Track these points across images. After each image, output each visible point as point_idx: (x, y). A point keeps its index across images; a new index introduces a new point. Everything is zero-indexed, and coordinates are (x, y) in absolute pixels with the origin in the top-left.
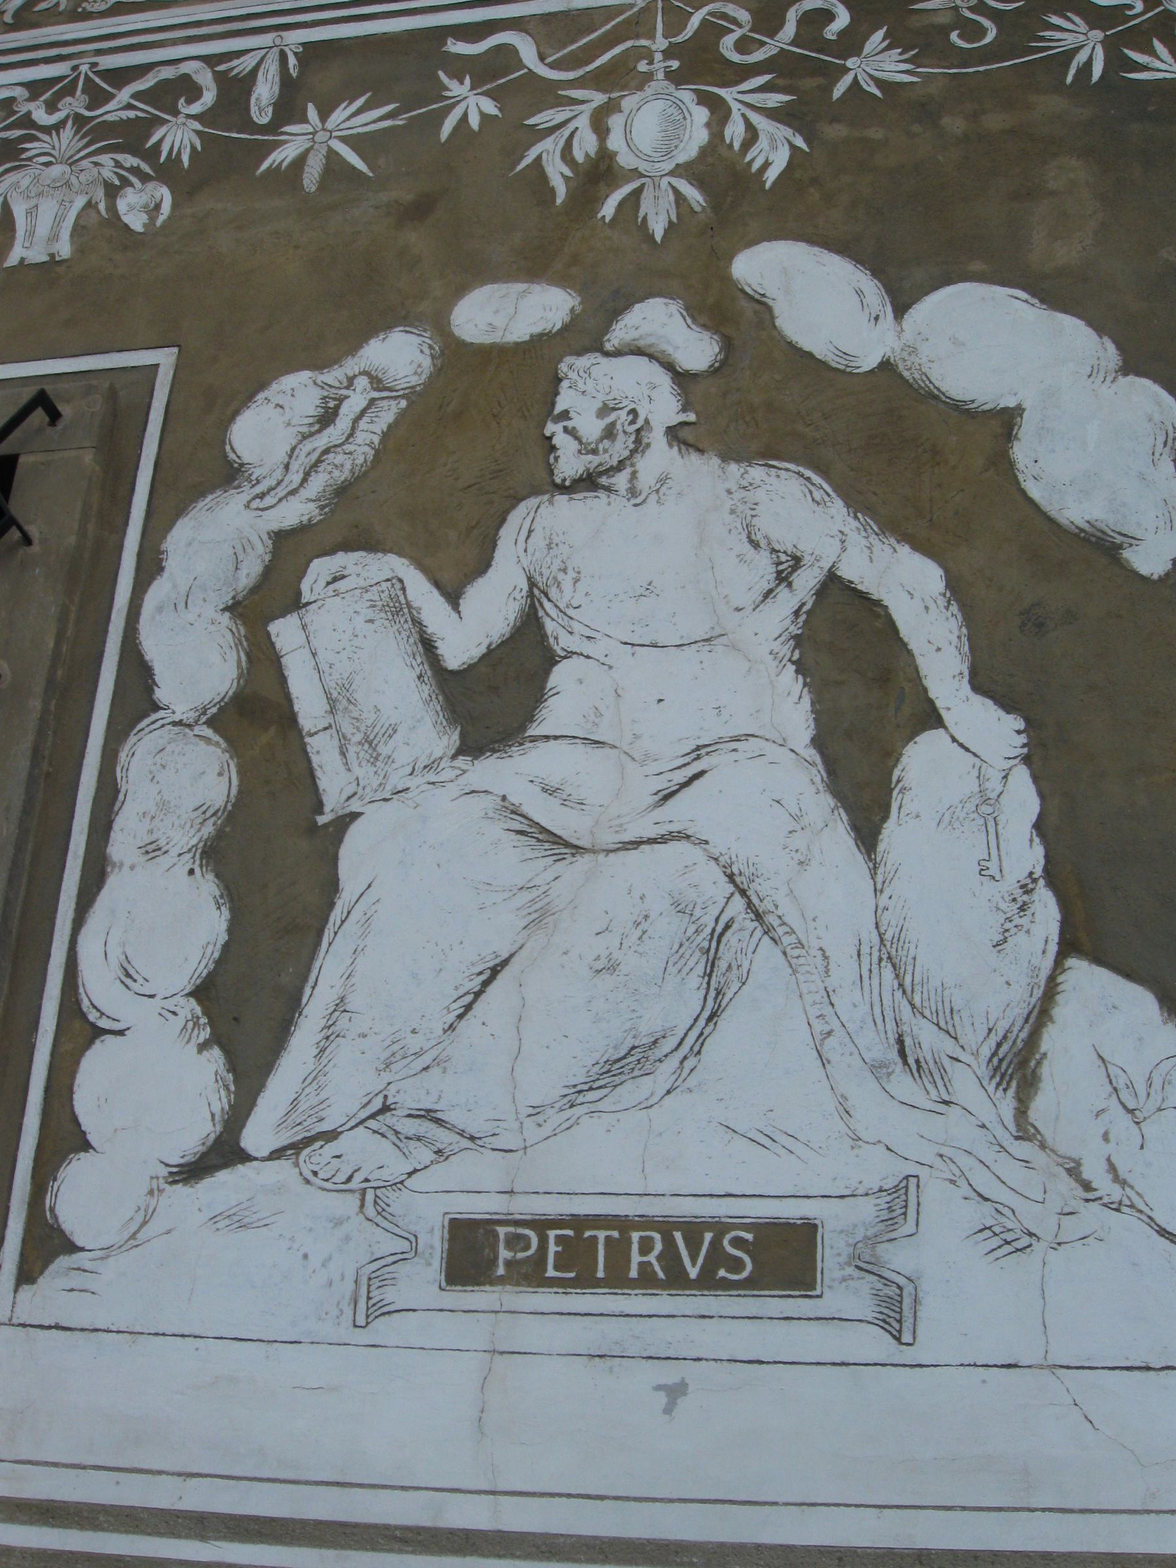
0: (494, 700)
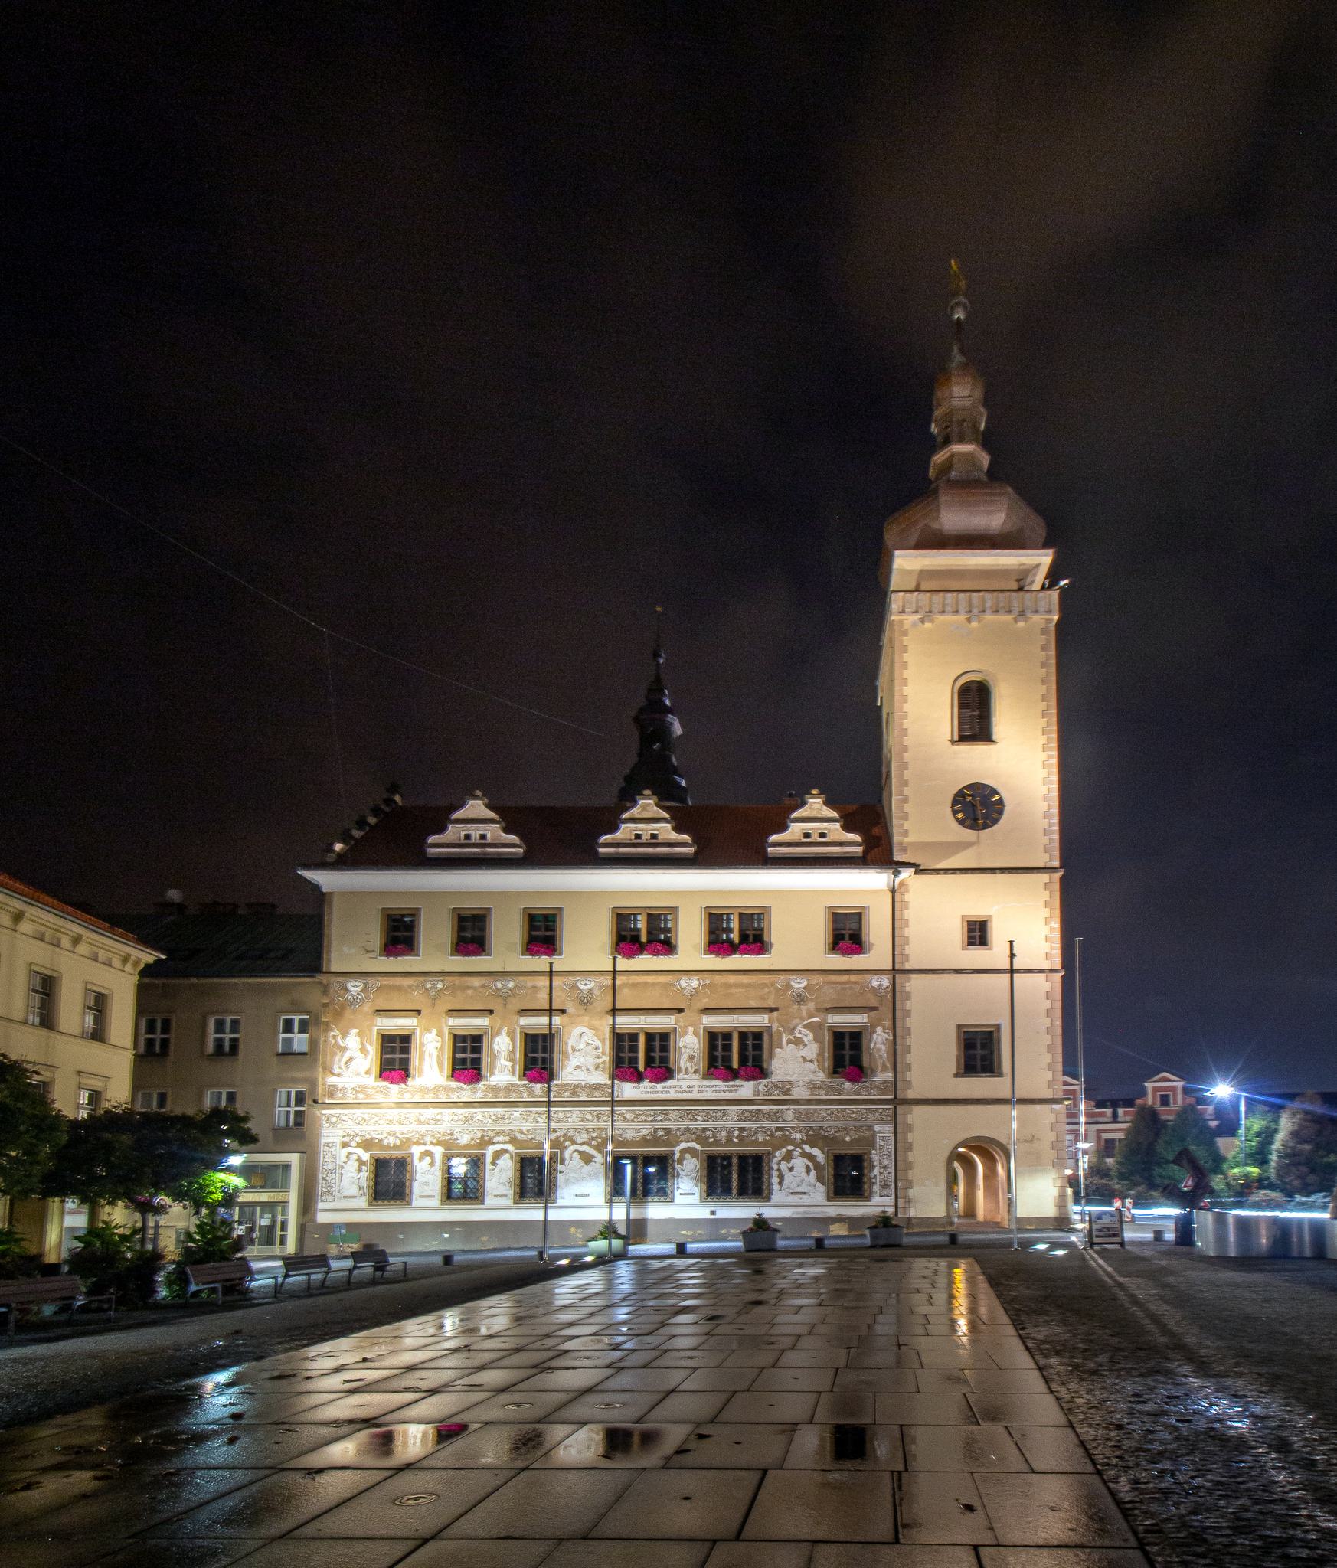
0: (791, 1169)
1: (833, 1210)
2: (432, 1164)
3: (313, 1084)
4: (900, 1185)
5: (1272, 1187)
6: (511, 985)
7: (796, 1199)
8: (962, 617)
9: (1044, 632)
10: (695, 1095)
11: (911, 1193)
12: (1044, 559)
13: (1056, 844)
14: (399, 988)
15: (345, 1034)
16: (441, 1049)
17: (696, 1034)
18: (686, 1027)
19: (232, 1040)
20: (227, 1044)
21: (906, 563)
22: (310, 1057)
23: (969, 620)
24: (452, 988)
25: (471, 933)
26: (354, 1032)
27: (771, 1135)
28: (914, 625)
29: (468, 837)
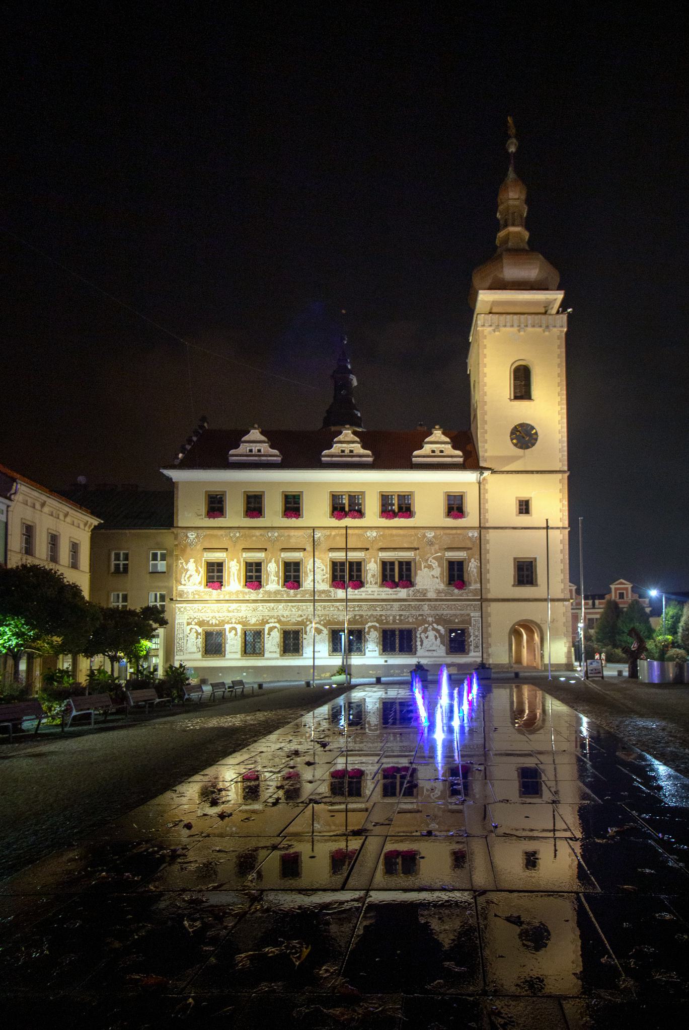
0: (427, 637)
1: (451, 659)
2: (236, 634)
3: (170, 590)
4: (484, 646)
5: (679, 647)
6: (276, 534)
7: (430, 654)
8: (515, 329)
9: (559, 338)
10: (376, 597)
11: (490, 650)
12: (559, 296)
13: (566, 458)
14: (216, 536)
15: (187, 562)
16: (240, 570)
17: (376, 562)
19: (124, 565)
20: (121, 566)
21: (485, 297)
22: (166, 574)
23: (519, 331)
24: (244, 536)
25: (254, 506)
26: (192, 560)
27: (416, 619)
28: (490, 333)
29: (251, 451)
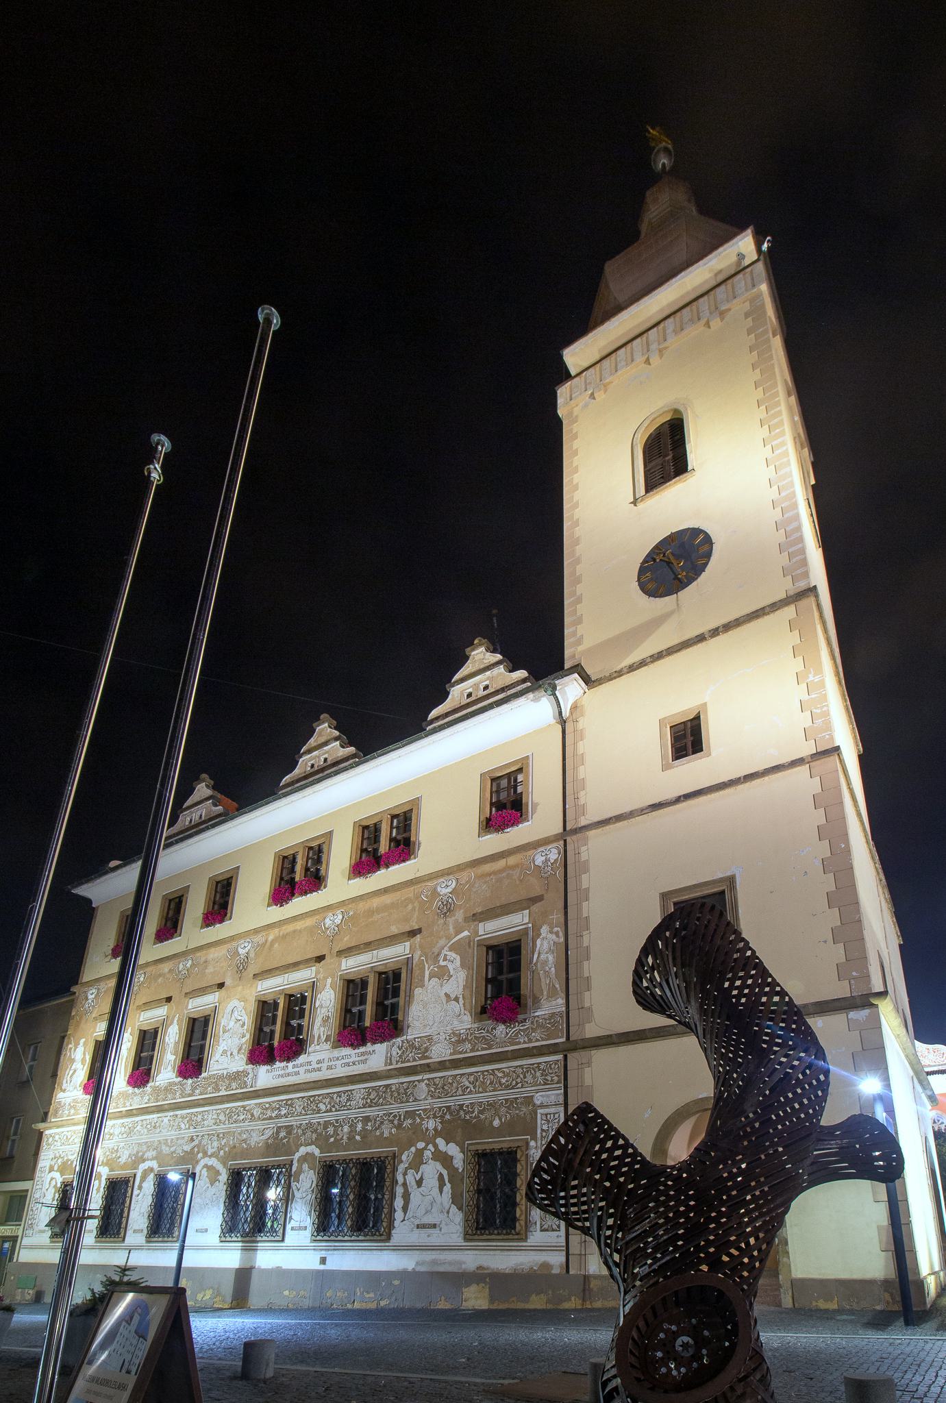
0: (419, 1183)
18: (325, 978)
27: (399, 1127)
